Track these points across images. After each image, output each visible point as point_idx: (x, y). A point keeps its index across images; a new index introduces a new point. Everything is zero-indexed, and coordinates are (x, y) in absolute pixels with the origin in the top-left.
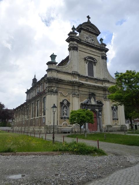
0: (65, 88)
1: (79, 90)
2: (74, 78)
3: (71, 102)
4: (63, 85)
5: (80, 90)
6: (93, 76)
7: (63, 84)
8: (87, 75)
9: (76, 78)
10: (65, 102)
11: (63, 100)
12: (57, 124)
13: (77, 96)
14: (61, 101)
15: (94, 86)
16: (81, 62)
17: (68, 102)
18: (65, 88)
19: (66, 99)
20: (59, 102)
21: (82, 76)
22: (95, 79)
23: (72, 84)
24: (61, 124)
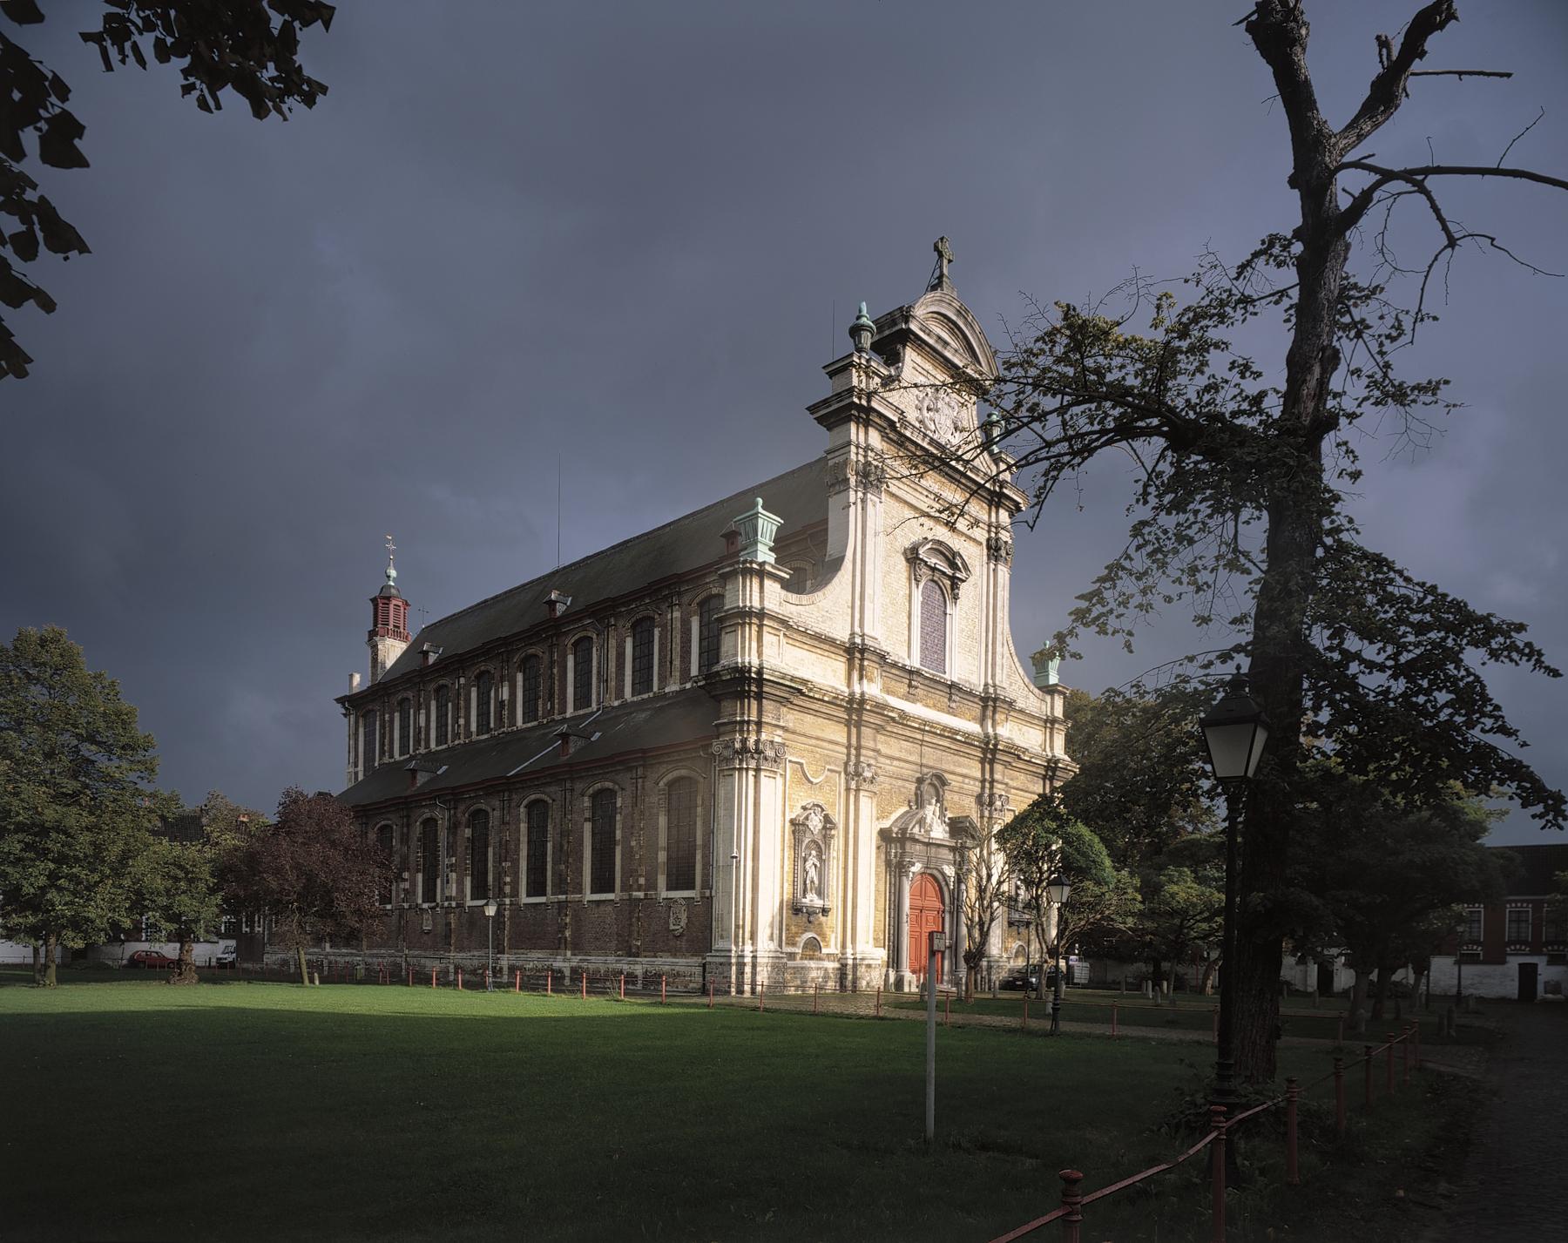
0: (817, 739)
1: (878, 751)
2: (861, 678)
3: (838, 818)
4: (809, 718)
5: (884, 750)
6: (941, 664)
7: (804, 710)
8: (915, 662)
9: (871, 680)
10: (816, 823)
11: (804, 808)
12: (780, 946)
13: (871, 787)
14: (795, 812)
15: (951, 734)
16: (888, 573)
17: (827, 819)
18: (817, 739)
19: (821, 803)
20: (788, 819)
21: (894, 665)
22: (953, 687)
23: (854, 710)
24: (794, 944)
